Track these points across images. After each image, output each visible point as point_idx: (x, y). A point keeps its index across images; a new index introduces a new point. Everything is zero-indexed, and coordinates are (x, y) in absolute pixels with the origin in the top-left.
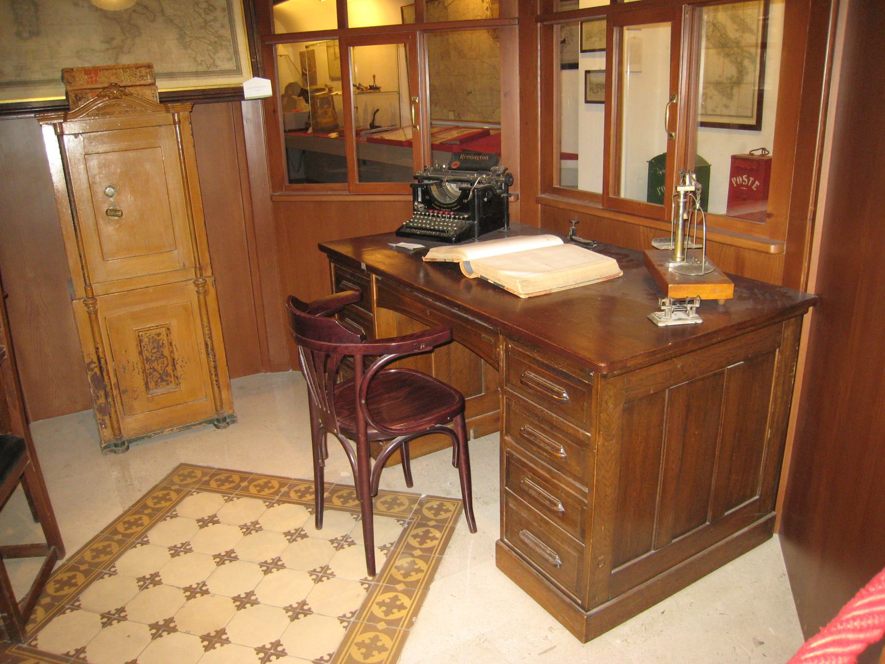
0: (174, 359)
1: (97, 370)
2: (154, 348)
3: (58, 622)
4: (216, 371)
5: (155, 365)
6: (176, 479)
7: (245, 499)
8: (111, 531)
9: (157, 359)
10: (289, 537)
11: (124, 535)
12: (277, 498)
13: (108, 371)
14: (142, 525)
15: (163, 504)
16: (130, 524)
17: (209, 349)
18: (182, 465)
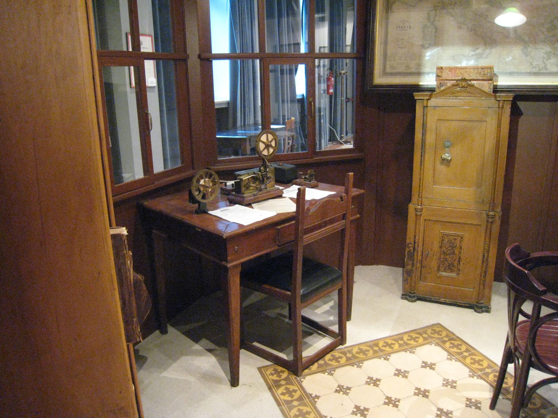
0: (460, 258)
1: (412, 249)
2: (450, 247)
3: (320, 376)
4: (485, 275)
5: (448, 257)
6: (429, 331)
7: (459, 364)
8: (374, 344)
9: (449, 254)
10: (468, 403)
11: (380, 349)
12: (480, 373)
13: (418, 251)
14: (417, 342)
15: (412, 342)
16: (387, 344)
17: (485, 260)
18: (439, 324)
